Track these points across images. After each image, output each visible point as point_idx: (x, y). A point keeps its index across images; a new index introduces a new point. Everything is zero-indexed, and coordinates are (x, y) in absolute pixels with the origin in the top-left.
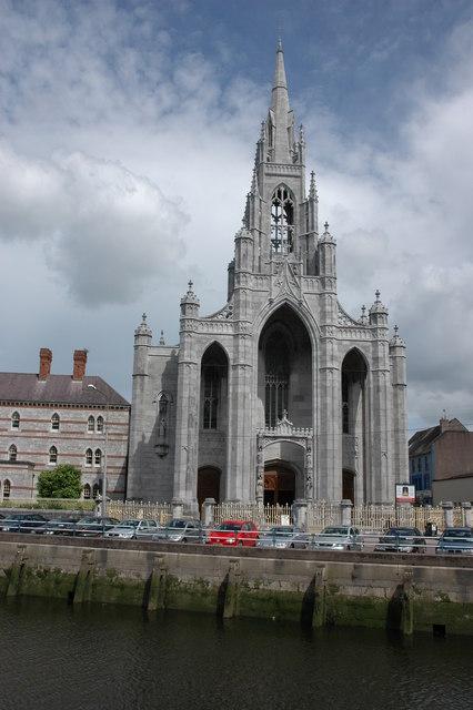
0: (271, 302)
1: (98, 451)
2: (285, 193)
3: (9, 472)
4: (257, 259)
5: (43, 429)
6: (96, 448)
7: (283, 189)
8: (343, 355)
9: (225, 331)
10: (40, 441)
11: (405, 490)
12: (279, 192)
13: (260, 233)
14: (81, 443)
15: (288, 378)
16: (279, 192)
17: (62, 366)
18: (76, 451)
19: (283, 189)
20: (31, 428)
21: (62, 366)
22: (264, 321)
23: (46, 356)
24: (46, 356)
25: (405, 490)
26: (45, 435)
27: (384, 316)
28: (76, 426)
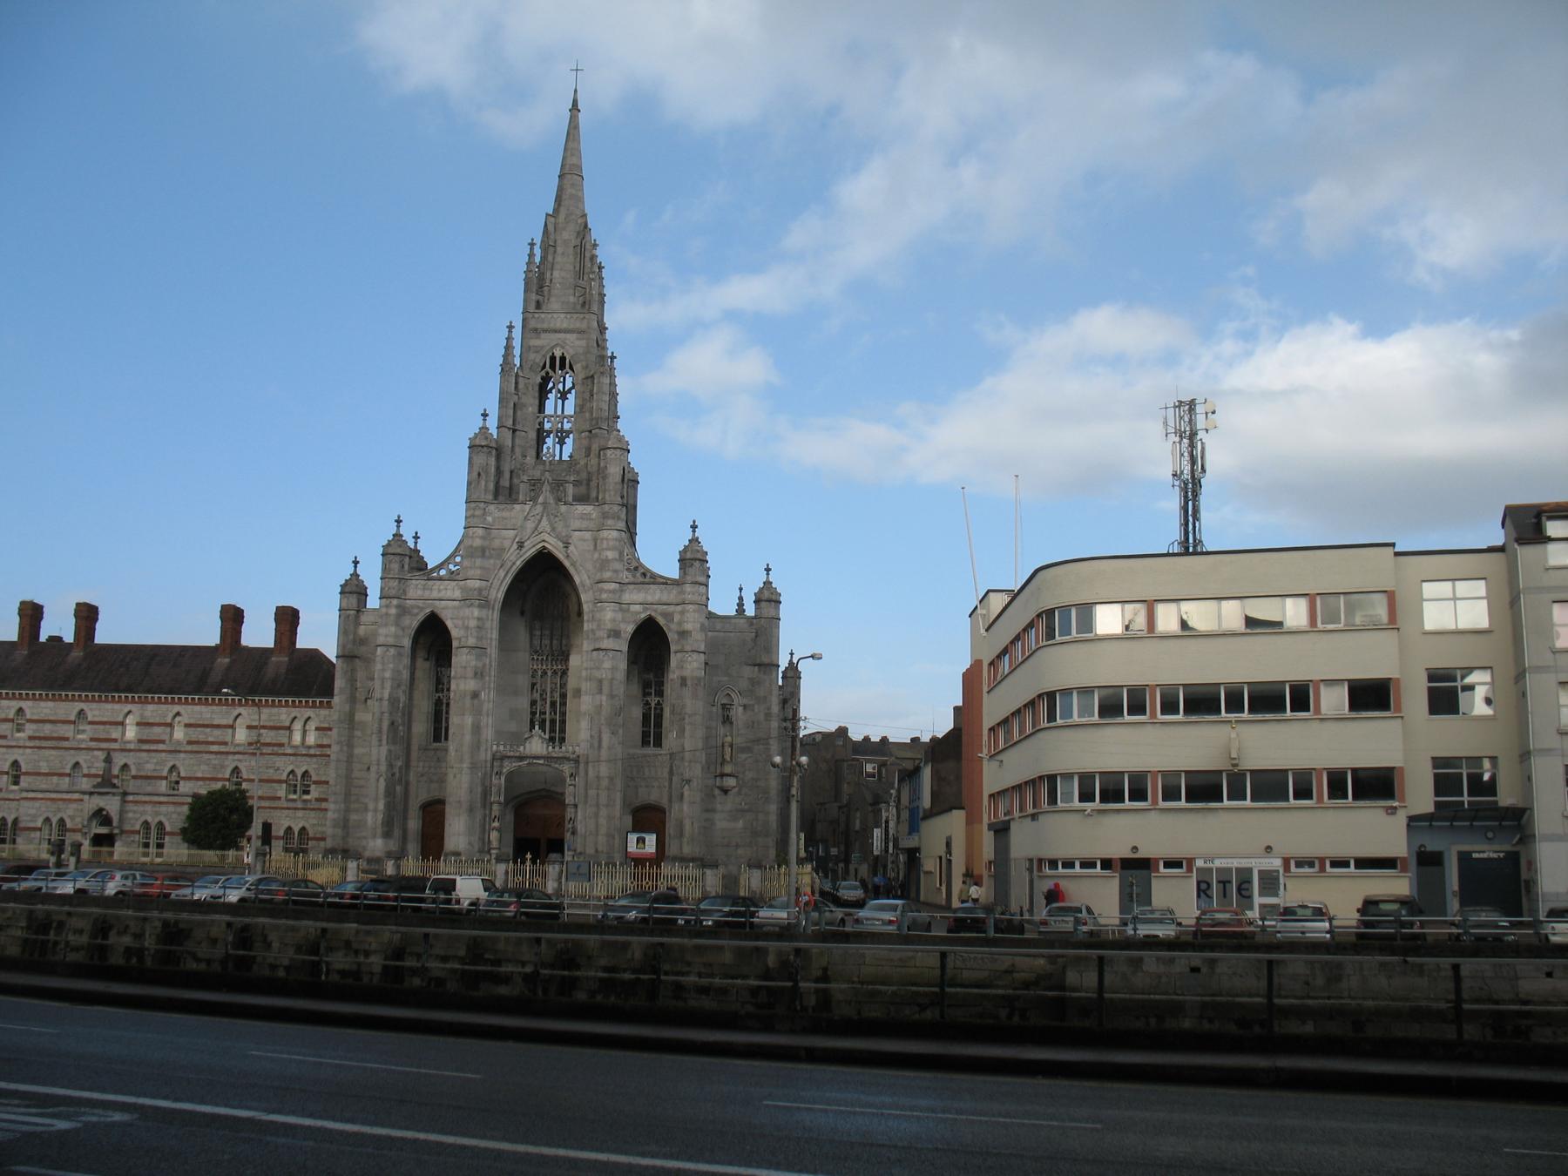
0: (521, 545)
1: (306, 774)
2: (563, 359)
3: (163, 809)
4: (507, 475)
5: (221, 739)
6: (303, 770)
7: (558, 354)
8: (630, 629)
9: (449, 594)
10: (215, 760)
11: (641, 841)
12: (553, 358)
13: (514, 431)
14: (280, 762)
15: (567, 660)
16: (553, 358)
17: (259, 633)
18: (271, 774)
19: (558, 354)
20: (202, 738)
21: (259, 633)
22: (508, 580)
23: (232, 618)
24: (232, 618)
25: (641, 841)
26: (223, 748)
27: (697, 564)
28: (272, 733)
